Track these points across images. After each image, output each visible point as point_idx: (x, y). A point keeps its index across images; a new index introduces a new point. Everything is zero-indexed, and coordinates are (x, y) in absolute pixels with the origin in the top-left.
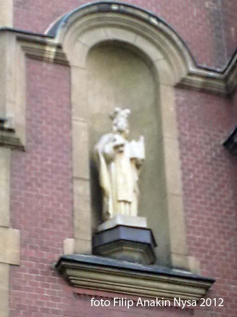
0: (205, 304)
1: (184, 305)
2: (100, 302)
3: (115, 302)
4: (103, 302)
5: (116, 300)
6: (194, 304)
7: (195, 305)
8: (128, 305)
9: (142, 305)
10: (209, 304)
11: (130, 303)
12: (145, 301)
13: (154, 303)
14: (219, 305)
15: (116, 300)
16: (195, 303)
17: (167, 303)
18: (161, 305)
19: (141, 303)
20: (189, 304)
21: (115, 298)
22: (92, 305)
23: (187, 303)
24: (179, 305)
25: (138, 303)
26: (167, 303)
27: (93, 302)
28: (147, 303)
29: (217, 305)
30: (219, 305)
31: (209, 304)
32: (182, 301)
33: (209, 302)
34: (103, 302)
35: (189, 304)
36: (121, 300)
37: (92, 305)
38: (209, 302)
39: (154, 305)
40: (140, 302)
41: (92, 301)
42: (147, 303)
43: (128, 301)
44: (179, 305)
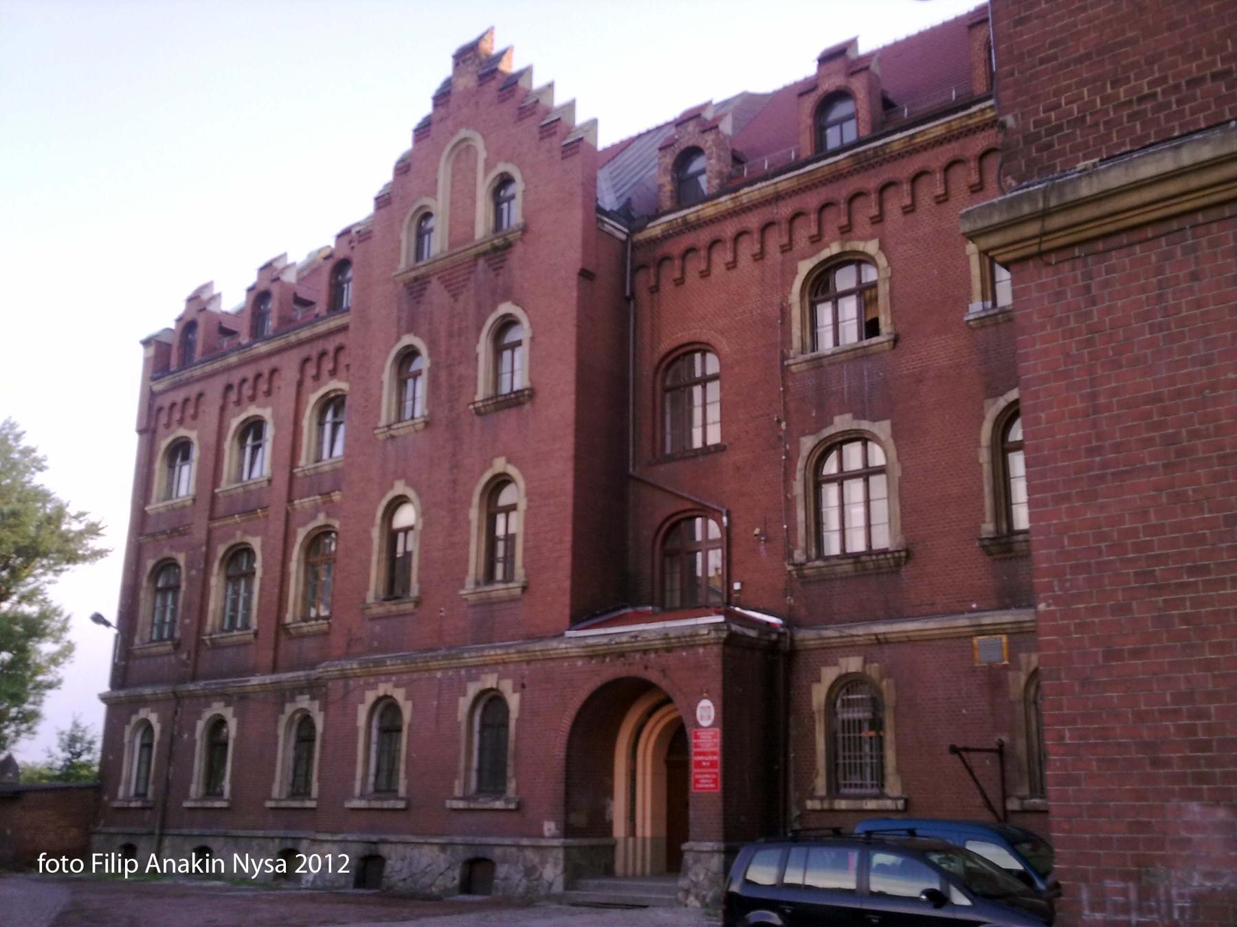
0: (306, 867)
1: (257, 871)
2: (61, 863)
3: (94, 863)
5: (98, 859)
6: (281, 868)
7: (284, 870)
8: (127, 870)
9: (159, 871)
10: (315, 866)
11: (131, 866)
12: (165, 862)
13: (187, 865)
14: (340, 871)
15: (98, 859)
16: (284, 865)
17: (218, 864)
18: (204, 869)
19: (157, 866)
20: (269, 869)
21: (94, 855)
22: (41, 871)
24: (246, 870)
25: (149, 866)
26: (218, 864)
27: (44, 863)
28: (169, 864)
29: (335, 867)
30: (340, 871)
31: (315, 867)
32: (253, 860)
34: (68, 864)
35: (269, 869)
36: (110, 858)
37: (41, 871)
39: (187, 870)
40: (153, 863)
41: (41, 860)
42: (169, 864)
43: (127, 862)
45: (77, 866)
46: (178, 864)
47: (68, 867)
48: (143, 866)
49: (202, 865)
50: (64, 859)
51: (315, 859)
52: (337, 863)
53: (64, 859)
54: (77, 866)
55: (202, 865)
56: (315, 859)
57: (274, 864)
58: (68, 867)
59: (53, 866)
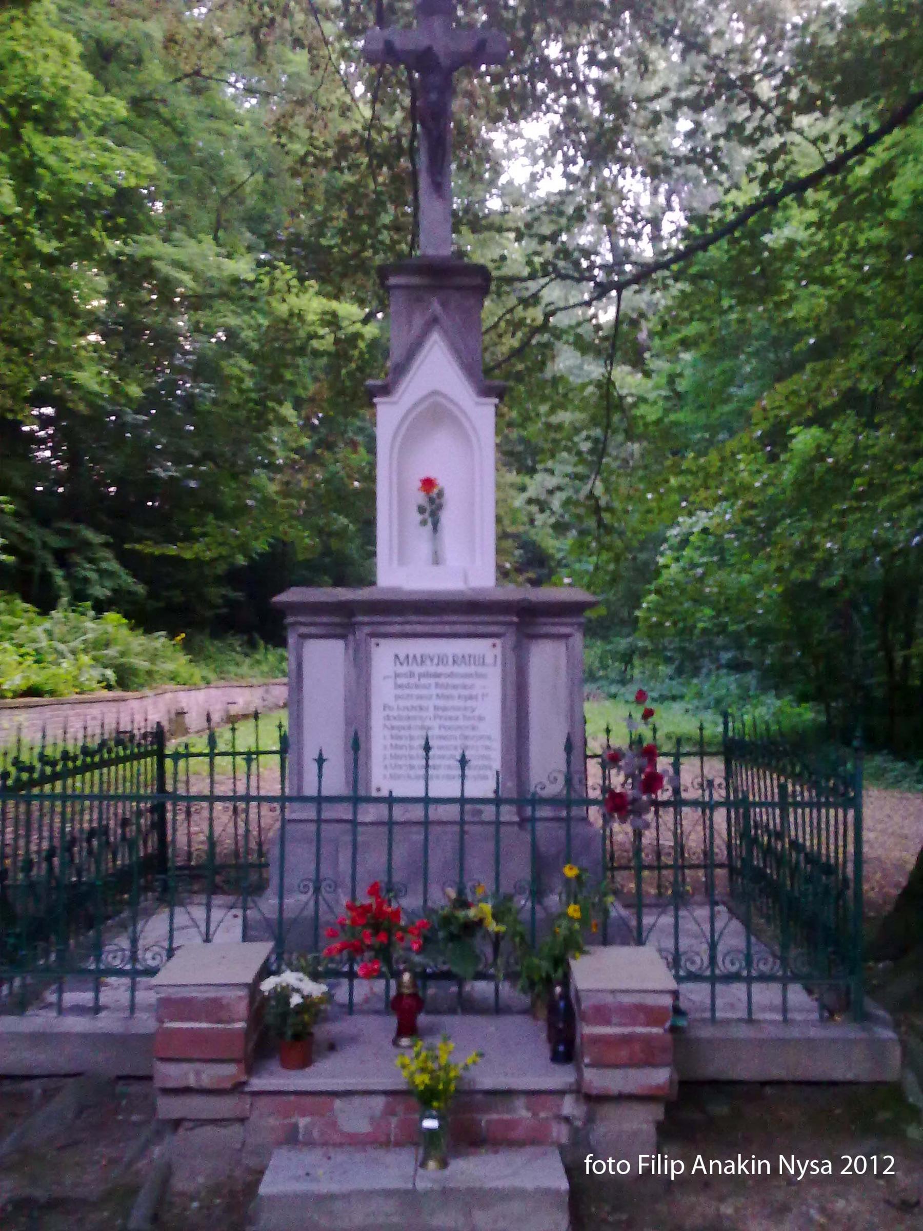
0: (851, 1169)
3: (641, 1165)
4: (614, 1165)
10: (860, 1169)
11: (678, 1167)
15: (644, 1160)
17: (764, 1165)
18: (750, 1170)
23: (809, 1167)
24: (792, 1172)
26: (764, 1165)
28: (716, 1165)
31: (860, 1169)
33: (860, 1162)
34: (614, 1165)
38: (860, 1162)
41: (587, 1161)
42: (716, 1165)
44: (792, 1172)
45: (623, 1167)
46: (724, 1165)
47: (614, 1169)
48: (689, 1167)
49: (748, 1167)
50: (610, 1161)
51: (861, 1161)
52: (883, 1164)
53: (610, 1161)
54: (623, 1167)
55: (748, 1167)
56: (861, 1161)
57: (820, 1165)
58: (614, 1169)
59: (599, 1167)
